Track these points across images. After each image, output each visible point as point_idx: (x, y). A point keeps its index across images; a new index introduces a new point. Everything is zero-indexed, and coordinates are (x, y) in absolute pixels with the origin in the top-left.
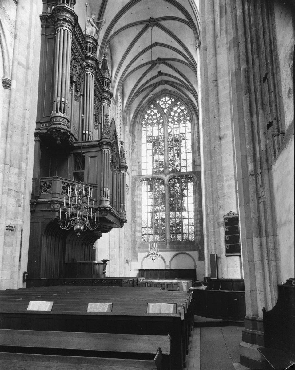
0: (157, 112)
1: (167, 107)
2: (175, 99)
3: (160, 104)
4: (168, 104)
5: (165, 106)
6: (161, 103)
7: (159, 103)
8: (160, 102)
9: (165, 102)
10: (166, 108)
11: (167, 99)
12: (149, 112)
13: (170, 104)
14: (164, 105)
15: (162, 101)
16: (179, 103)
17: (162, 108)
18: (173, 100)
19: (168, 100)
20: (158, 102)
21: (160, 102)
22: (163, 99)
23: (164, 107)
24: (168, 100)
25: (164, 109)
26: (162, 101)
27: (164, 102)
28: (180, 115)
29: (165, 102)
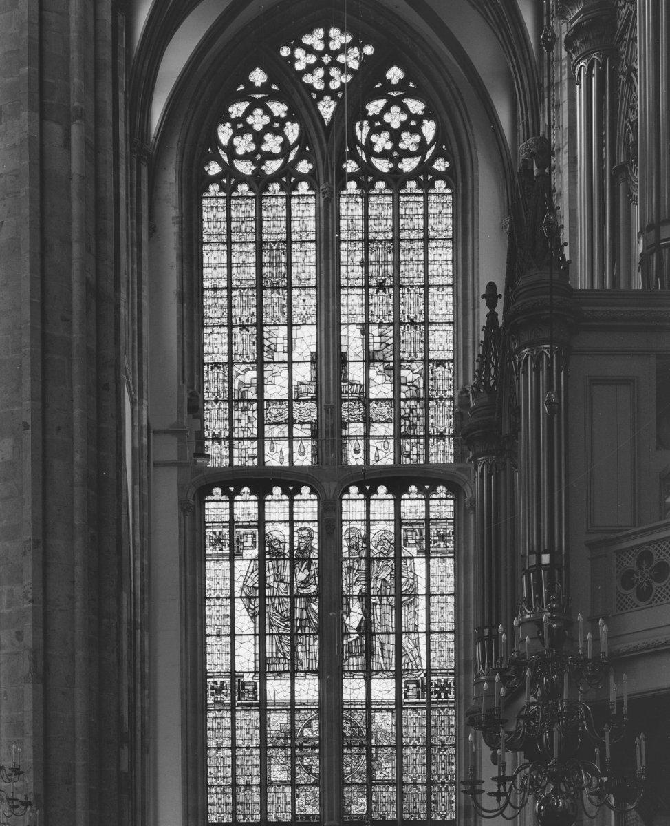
0: (283, 115)
1: (335, 85)
2: (375, 47)
3: (299, 66)
4: (343, 68)
5: (327, 79)
6: (303, 60)
7: (292, 59)
8: (299, 53)
9: (326, 59)
10: (332, 94)
11: (339, 38)
12: (237, 110)
13: (351, 71)
14: (320, 73)
15: (309, 50)
16: (395, 74)
17: (310, 88)
18: (369, 50)
19: (344, 49)
20: (285, 52)
21: (299, 53)
22: (315, 39)
23: (319, 86)
24: (344, 49)
25: (321, 94)
26: (309, 50)
27: (319, 54)
28: (401, 145)
29: (326, 59)
